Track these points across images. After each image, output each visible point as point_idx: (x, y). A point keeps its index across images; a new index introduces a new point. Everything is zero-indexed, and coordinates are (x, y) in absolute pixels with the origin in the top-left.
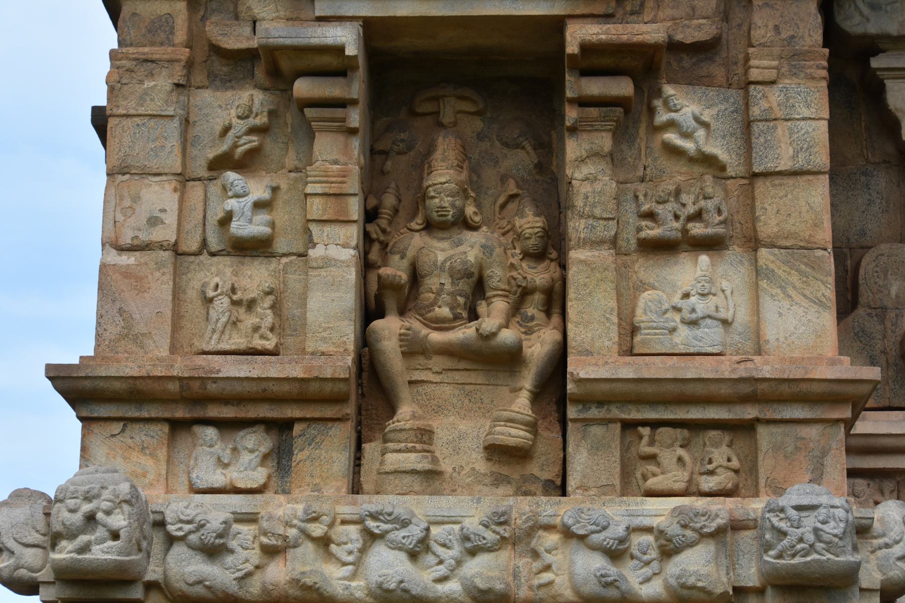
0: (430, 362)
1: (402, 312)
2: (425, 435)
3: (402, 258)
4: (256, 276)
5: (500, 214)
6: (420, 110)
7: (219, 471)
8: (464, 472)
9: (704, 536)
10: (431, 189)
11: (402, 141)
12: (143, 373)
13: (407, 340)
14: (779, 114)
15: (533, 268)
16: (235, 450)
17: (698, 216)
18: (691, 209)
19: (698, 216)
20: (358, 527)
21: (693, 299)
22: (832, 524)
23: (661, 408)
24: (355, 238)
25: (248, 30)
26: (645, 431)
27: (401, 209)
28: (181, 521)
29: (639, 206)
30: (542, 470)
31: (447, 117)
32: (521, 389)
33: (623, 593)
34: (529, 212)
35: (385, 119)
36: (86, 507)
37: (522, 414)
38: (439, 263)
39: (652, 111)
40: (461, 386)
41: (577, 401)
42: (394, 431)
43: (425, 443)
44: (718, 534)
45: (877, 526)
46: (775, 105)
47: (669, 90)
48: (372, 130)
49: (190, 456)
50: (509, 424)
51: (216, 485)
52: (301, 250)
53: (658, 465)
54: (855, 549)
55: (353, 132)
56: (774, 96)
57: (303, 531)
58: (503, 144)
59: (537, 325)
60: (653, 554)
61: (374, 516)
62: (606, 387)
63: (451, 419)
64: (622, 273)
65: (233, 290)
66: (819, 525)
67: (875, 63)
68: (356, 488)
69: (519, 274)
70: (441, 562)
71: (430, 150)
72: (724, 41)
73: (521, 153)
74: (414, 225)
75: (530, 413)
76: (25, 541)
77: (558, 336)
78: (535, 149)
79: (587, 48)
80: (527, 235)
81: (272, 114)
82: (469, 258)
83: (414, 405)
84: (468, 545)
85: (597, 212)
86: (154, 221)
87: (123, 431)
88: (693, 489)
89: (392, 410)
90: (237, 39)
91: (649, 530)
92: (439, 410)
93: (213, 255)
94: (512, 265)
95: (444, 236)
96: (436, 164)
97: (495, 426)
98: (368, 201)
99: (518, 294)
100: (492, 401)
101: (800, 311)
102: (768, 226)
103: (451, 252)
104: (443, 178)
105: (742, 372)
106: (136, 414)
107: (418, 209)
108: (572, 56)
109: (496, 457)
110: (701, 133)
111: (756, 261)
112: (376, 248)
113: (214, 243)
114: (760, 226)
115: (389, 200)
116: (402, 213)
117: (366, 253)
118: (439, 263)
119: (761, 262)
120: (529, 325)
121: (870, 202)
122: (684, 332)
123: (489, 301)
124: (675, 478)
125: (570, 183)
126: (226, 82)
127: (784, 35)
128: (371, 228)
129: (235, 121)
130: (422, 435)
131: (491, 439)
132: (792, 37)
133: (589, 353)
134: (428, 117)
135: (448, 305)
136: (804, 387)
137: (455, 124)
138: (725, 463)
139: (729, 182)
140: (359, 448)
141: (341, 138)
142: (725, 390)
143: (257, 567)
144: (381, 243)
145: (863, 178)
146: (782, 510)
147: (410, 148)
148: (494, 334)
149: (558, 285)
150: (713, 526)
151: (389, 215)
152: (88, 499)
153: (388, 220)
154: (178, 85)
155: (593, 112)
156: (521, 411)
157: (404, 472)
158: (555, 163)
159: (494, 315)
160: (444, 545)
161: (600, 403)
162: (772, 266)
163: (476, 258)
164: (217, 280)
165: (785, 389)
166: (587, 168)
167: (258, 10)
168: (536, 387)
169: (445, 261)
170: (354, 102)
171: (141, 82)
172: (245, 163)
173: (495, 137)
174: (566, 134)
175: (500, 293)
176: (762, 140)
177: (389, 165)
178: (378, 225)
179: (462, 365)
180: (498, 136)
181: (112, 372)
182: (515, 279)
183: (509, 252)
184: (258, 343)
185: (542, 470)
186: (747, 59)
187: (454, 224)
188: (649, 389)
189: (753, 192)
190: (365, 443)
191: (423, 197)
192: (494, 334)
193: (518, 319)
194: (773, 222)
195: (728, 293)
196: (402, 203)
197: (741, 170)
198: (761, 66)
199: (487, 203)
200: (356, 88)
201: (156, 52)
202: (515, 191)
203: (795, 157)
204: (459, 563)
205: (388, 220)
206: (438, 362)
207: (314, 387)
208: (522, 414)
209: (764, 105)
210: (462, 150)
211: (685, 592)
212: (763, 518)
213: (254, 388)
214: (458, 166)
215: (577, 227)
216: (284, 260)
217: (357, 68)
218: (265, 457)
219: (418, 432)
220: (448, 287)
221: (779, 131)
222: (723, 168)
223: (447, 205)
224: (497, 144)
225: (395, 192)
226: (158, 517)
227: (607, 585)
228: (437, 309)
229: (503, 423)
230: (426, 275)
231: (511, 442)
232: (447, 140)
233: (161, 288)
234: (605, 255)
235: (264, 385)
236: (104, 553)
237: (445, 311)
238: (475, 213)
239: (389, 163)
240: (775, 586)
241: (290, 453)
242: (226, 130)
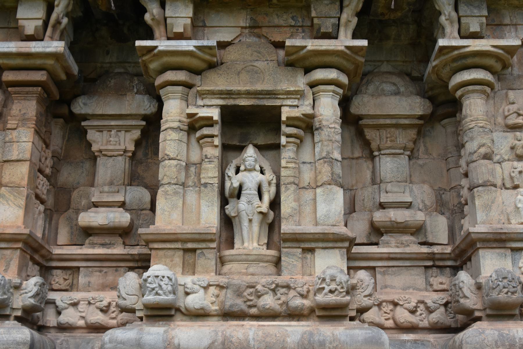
14: (15, 140)
46: (14, 137)
56: (15, 133)
101: (12, 209)
121: (83, 172)
127: (22, 113)
132: (25, 113)
145: (81, 164)
162: (5, 193)
194: (7, 178)
203: (18, 155)
209: (10, 137)
221: (14, 146)
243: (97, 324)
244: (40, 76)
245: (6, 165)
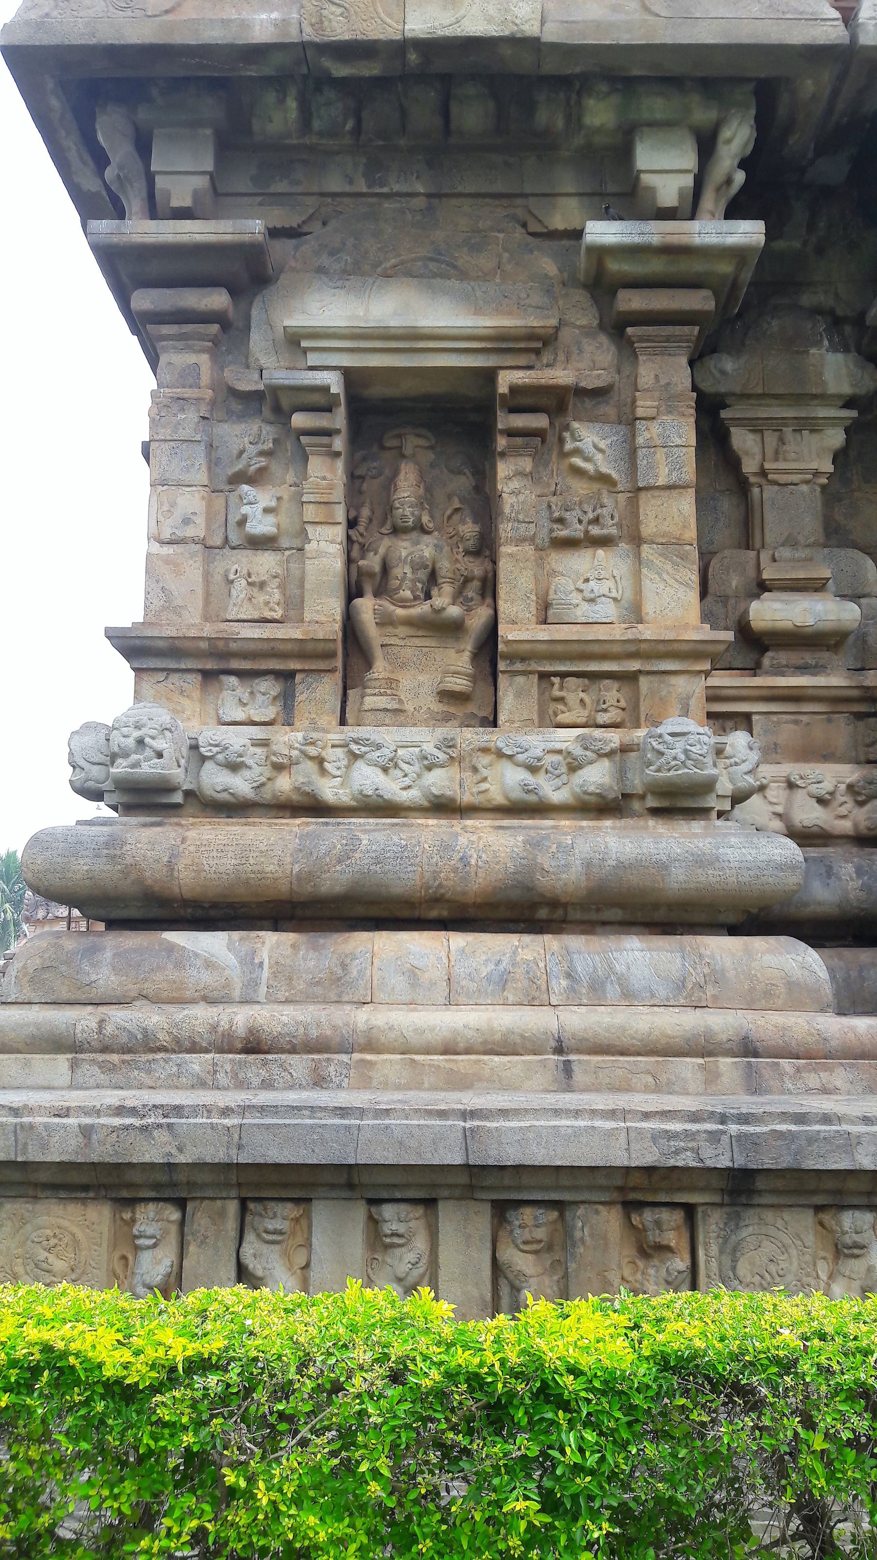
1: (377, 594)
2: (391, 683)
4: (266, 563)
6: (388, 445)
7: (240, 709)
9: (601, 755)
12: (180, 635)
14: (658, 443)
16: (252, 693)
17: (596, 521)
18: (591, 516)
19: (596, 521)
20: (346, 749)
21: (592, 583)
22: (698, 747)
23: (568, 663)
25: (256, 376)
26: (556, 680)
28: (211, 745)
29: (551, 513)
31: (408, 451)
33: (540, 798)
36: (137, 734)
39: (561, 441)
41: (505, 657)
44: (610, 755)
45: (728, 750)
46: (655, 436)
47: (575, 425)
49: (218, 698)
51: (238, 719)
52: (300, 546)
53: (566, 704)
54: (715, 765)
55: (337, 454)
56: (655, 429)
57: (302, 752)
60: (564, 769)
61: (356, 741)
62: (527, 647)
64: (540, 563)
65: (249, 575)
66: (689, 747)
67: (724, 414)
68: (343, 722)
70: (406, 776)
71: (396, 473)
72: (616, 388)
74: (384, 530)
76: (92, 760)
77: (490, 612)
79: (515, 390)
81: (275, 441)
84: (426, 762)
85: (521, 517)
86: (186, 521)
87: (166, 678)
88: (591, 722)
89: (368, 664)
90: (248, 383)
91: (559, 752)
92: (403, 666)
93: (233, 548)
94: (457, 560)
101: (672, 591)
102: (648, 528)
104: (407, 489)
105: (630, 635)
106: (176, 666)
108: (503, 395)
110: (599, 457)
111: (639, 554)
112: (356, 547)
113: (234, 539)
114: (643, 528)
115: (365, 512)
116: (375, 522)
119: (643, 555)
121: (717, 520)
122: (585, 606)
124: (577, 714)
126: (241, 417)
127: (662, 382)
128: (351, 532)
129: (247, 445)
131: (442, 687)
132: (668, 384)
133: (514, 622)
136: (676, 646)
137: (414, 456)
138: (616, 704)
139: (620, 495)
140: (345, 695)
141: (328, 460)
142: (616, 649)
143: (269, 779)
144: (360, 544)
146: (660, 736)
147: (380, 474)
149: (490, 575)
150: (608, 749)
152: (138, 727)
154: (204, 418)
155: (519, 440)
160: (408, 763)
161: (523, 659)
162: (651, 557)
164: (236, 566)
165: (661, 648)
166: (514, 483)
167: (264, 361)
170: (338, 432)
171: (175, 415)
172: (254, 479)
174: (498, 458)
176: (645, 462)
177: (365, 486)
179: (420, 633)
181: (156, 634)
184: (268, 614)
186: (634, 401)
187: (413, 529)
188: (559, 648)
189: (637, 502)
191: (392, 508)
192: (444, 609)
193: (461, 599)
194: (653, 524)
195: (618, 578)
197: (628, 486)
198: (644, 406)
200: (339, 419)
201: (188, 393)
202: (458, 506)
204: (419, 776)
206: (402, 631)
207: (310, 647)
211: (587, 797)
212: (645, 743)
213: (266, 646)
215: (505, 529)
216: (287, 553)
218: (275, 698)
220: (409, 575)
221: (658, 456)
222: (614, 483)
226: (193, 742)
227: (528, 792)
231: (457, 688)
233: (194, 571)
234: (529, 550)
235: (272, 644)
236: (149, 768)
237: (408, 594)
239: (365, 485)
240: (654, 793)
241: (293, 696)
242: (241, 453)
243: (815, 829)
244: (700, 301)
245: (643, 495)
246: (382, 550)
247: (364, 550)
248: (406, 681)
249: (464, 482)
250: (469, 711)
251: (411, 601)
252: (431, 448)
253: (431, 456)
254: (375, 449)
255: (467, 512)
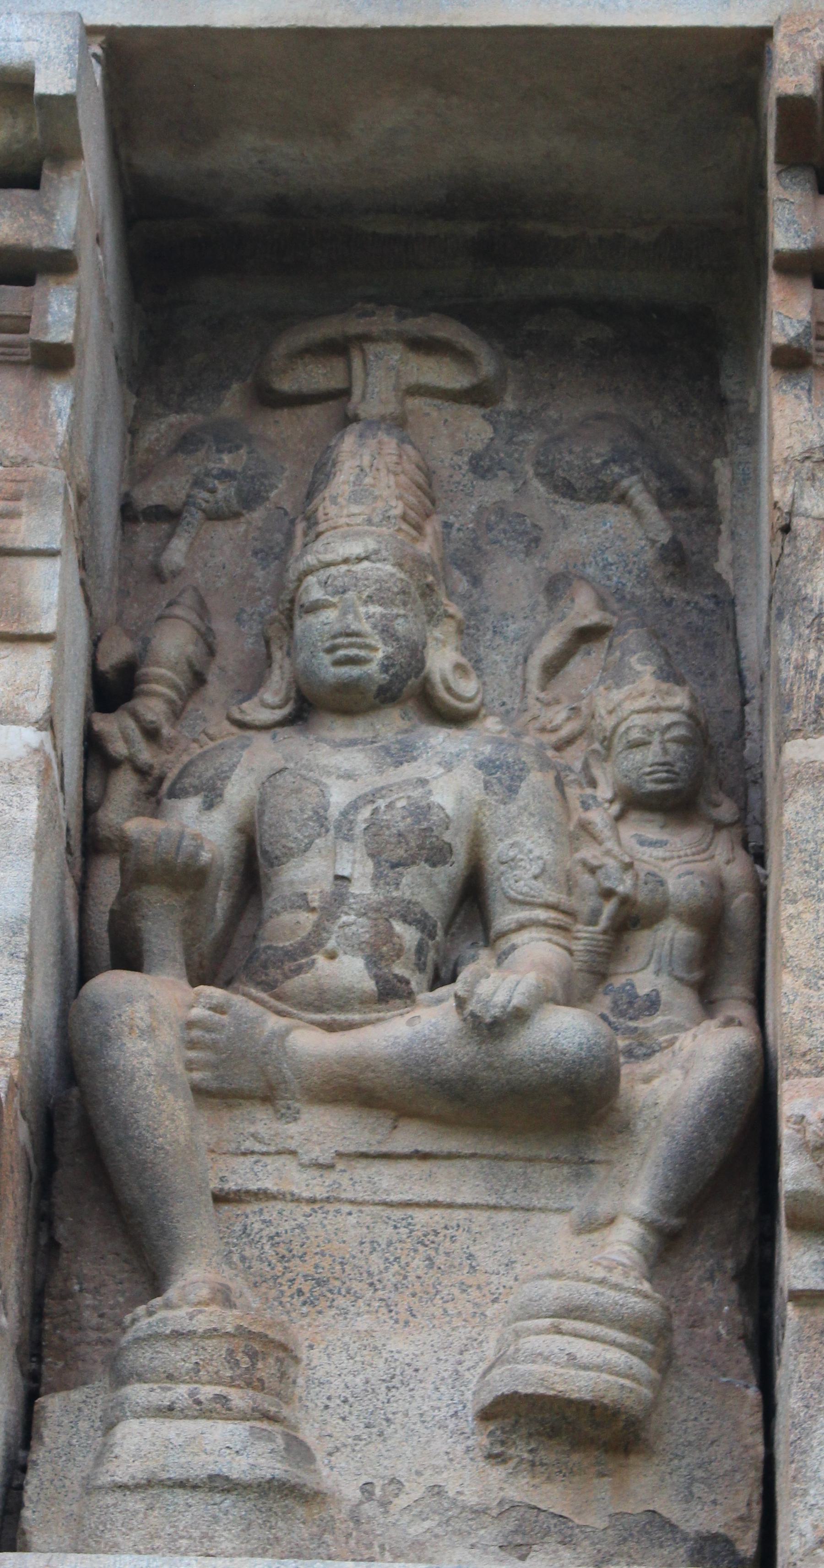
0: (293, 1128)
2: (262, 1366)
3: (209, 806)
5: (543, 689)
6: (286, 385)
8: (402, 1501)
10: (311, 579)
11: (226, 475)
13: (213, 1046)
15: (653, 844)
24: (44, 692)
27: (212, 677)
30: (689, 1497)
32: (611, 1221)
34: (644, 673)
35: (173, 418)
37: (616, 1287)
38: (334, 813)
40: (398, 1214)
42: (154, 1337)
43: (260, 1386)
48: (130, 448)
50: (568, 1324)
55: (54, 360)
58: (556, 489)
59: (671, 1027)
63: (363, 1323)
69: (608, 853)
71: (321, 472)
73: (614, 518)
75: (646, 1286)
78: (662, 506)
80: (635, 734)
82: (436, 799)
83: (228, 1272)
89: (152, 1275)
92: (318, 1291)
94: (585, 827)
95: (352, 734)
96: (332, 510)
97: (518, 1335)
98: (102, 645)
99: (604, 921)
100: (510, 1264)
103: (380, 781)
107: (269, 657)
109: (520, 1450)
112: (124, 785)
115: (173, 644)
116: (215, 688)
117: (89, 810)
118: (334, 813)
120: (640, 1024)
123: (503, 945)
125: (786, 529)
128: (105, 724)
130: (253, 1356)
131: (503, 1382)
134: (313, 410)
135: (357, 948)
144: (142, 772)
147: (250, 499)
148: (519, 1016)
149: (740, 904)
151: (174, 687)
153: (170, 702)
156: (616, 1277)
157: (182, 1484)
158: (725, 552)
159: (517, 970)
163: (460, 799)
168: (666, 1208)
169: (354, 807)
170: (61, 264)
173: (530, 470)
175: (542, 914)
177: (177, 552)
178: (135, 716)
179: (409, 1137)
180: (538, 463)
182: (593, 870)
183: (573, 792)
185: (689, 1497)
187: (386, 696)
190: (53, 1390)
191: (291, 610)
192: (519, 1016)
196: (219, 660)
199: (500, 659)
202: (594, 617)
205: (170, 702)
206: (322, 1129)
208: (616, 1287)
210: (421, 479)
214: (404, 518)
217: (77, 154)
219: (240, 1344)
220: (362, 888)
223: (366, 627)
224: (538, 487)
225: (193, 617)
228: (320, 959)
229: (547, 1322)
230: (290, 854)
231: (578, 1385)
232: (372, 443)
238: (458, 667)
246: (239, 791)
247: (154, 793)
248: (333, 1355)
249: (619, 534)
250: (634, 1507)
251: (364, 1001)
252: (478, 396)
253: (475, 428)
254: (231, 403)
255: (632, 636)
